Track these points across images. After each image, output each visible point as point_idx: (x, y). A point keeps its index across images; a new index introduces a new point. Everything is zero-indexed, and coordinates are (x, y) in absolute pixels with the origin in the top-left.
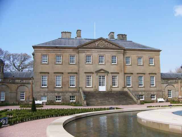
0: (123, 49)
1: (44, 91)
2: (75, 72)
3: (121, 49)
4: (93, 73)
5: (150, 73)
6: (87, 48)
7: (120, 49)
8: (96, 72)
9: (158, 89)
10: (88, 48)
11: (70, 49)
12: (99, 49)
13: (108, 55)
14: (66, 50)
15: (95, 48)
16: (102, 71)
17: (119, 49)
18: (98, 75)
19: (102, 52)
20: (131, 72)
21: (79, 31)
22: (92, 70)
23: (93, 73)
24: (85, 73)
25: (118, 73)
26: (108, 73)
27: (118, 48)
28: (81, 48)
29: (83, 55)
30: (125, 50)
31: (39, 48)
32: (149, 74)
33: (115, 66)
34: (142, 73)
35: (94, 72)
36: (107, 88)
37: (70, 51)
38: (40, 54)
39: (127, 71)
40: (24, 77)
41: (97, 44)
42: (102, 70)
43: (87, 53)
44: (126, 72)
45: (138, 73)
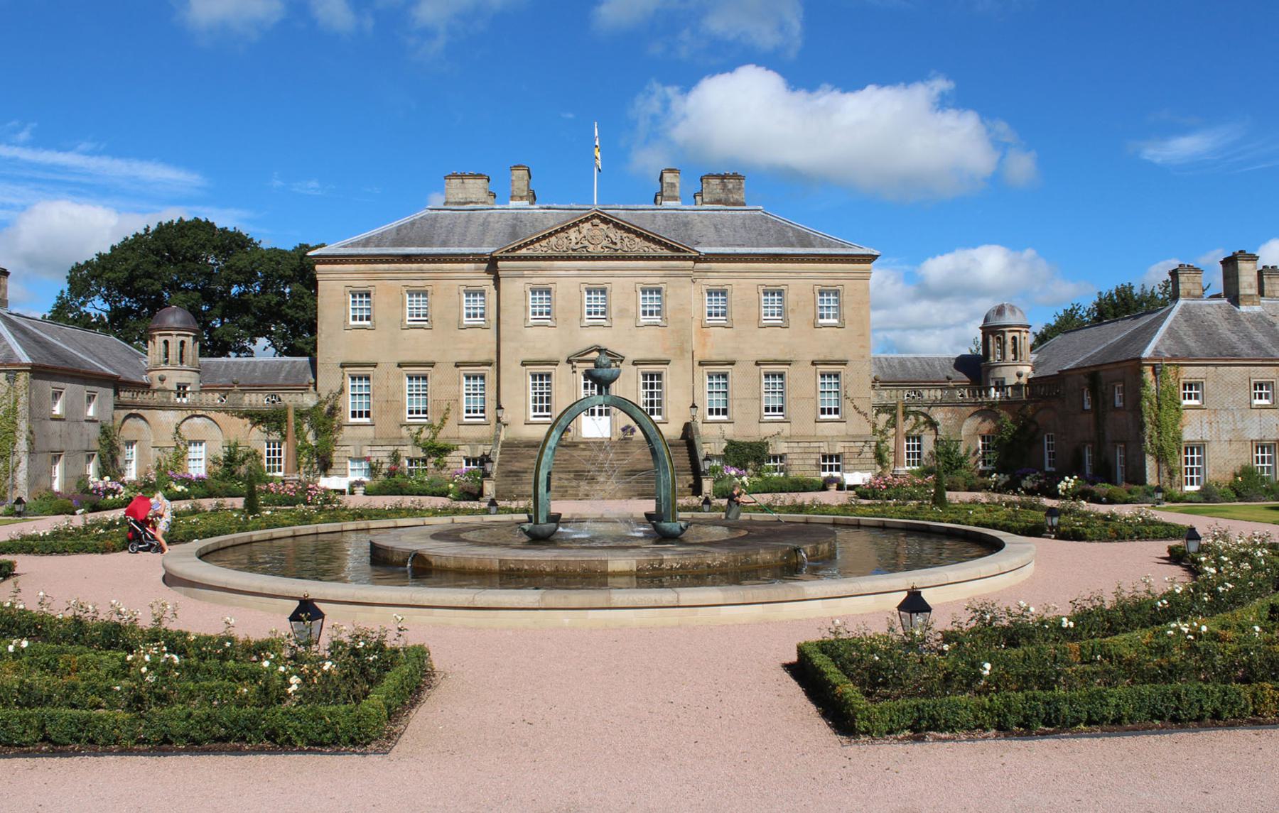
0: (690, 258)
1: (361, 440)
2: (483, 357)
3: (685, 259)
4: (556, 363)
5: (821, 357)
6: (532, 258)
7: (678, 258)
9: (852, 431)
10: (538, 258)
11: (462, 262)
15: (569, 258)
17: (672, 258)
19: (598, 273)
20: (730, 357)
23: (555, 363)
24: (524, 364)
25: (667, 362)
28: (507, 259)
31: (335, 263)
32: (813, 363)
37: (462, 271)
40: (280, 382)
43: (534, 280)
44: (707, 358)
45: (760, 358)
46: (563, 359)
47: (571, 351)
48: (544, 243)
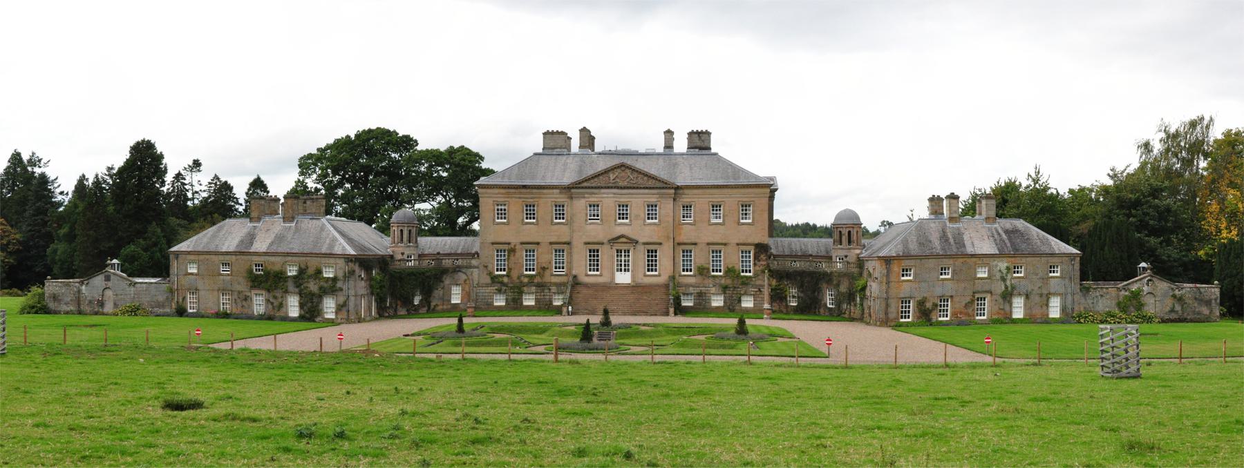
8: (609, 241)
12: (618, 188)
13: (638, 202)
16: (624, 240)
20: (693, 241)
21: (585, 132)
27: (659, 185)
30: (677, 188)
33: (652, 227)
36: (633, 277)
38: (490, 201)
39: (683, 239)
41: (612, 176)
47: (610, 237)
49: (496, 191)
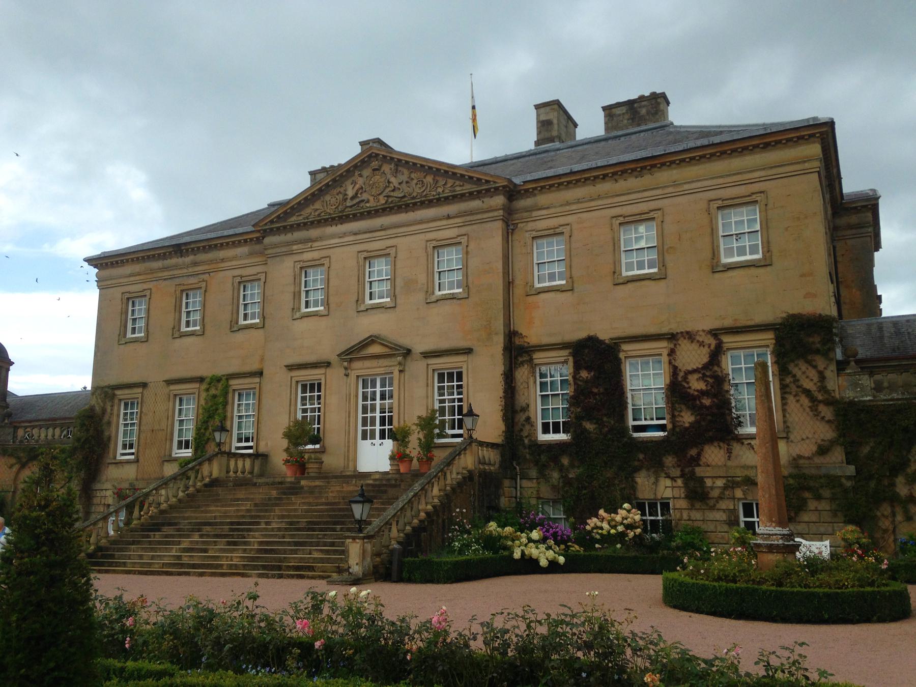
4: (328, 364)
5: (728, 323)
7: (478, 195)
14: (222, 254)
16: (375, 349)
18: (353, 374)
22: (328, 350)
23: (328, 364)
24: (291, 368)
25: (468, 351)
26: (408, 352)
27: (468, 188)
28: (272, 232)
29: (283, 270)
30: (512, 193)
33: (447, 307)
34: (653, 330)
35: (333, 358)
37: (234, 258)
42: (372, 340)
46: (333, 358)
47: (343, 347)
48: (318, 205)
49: (128, 269)
